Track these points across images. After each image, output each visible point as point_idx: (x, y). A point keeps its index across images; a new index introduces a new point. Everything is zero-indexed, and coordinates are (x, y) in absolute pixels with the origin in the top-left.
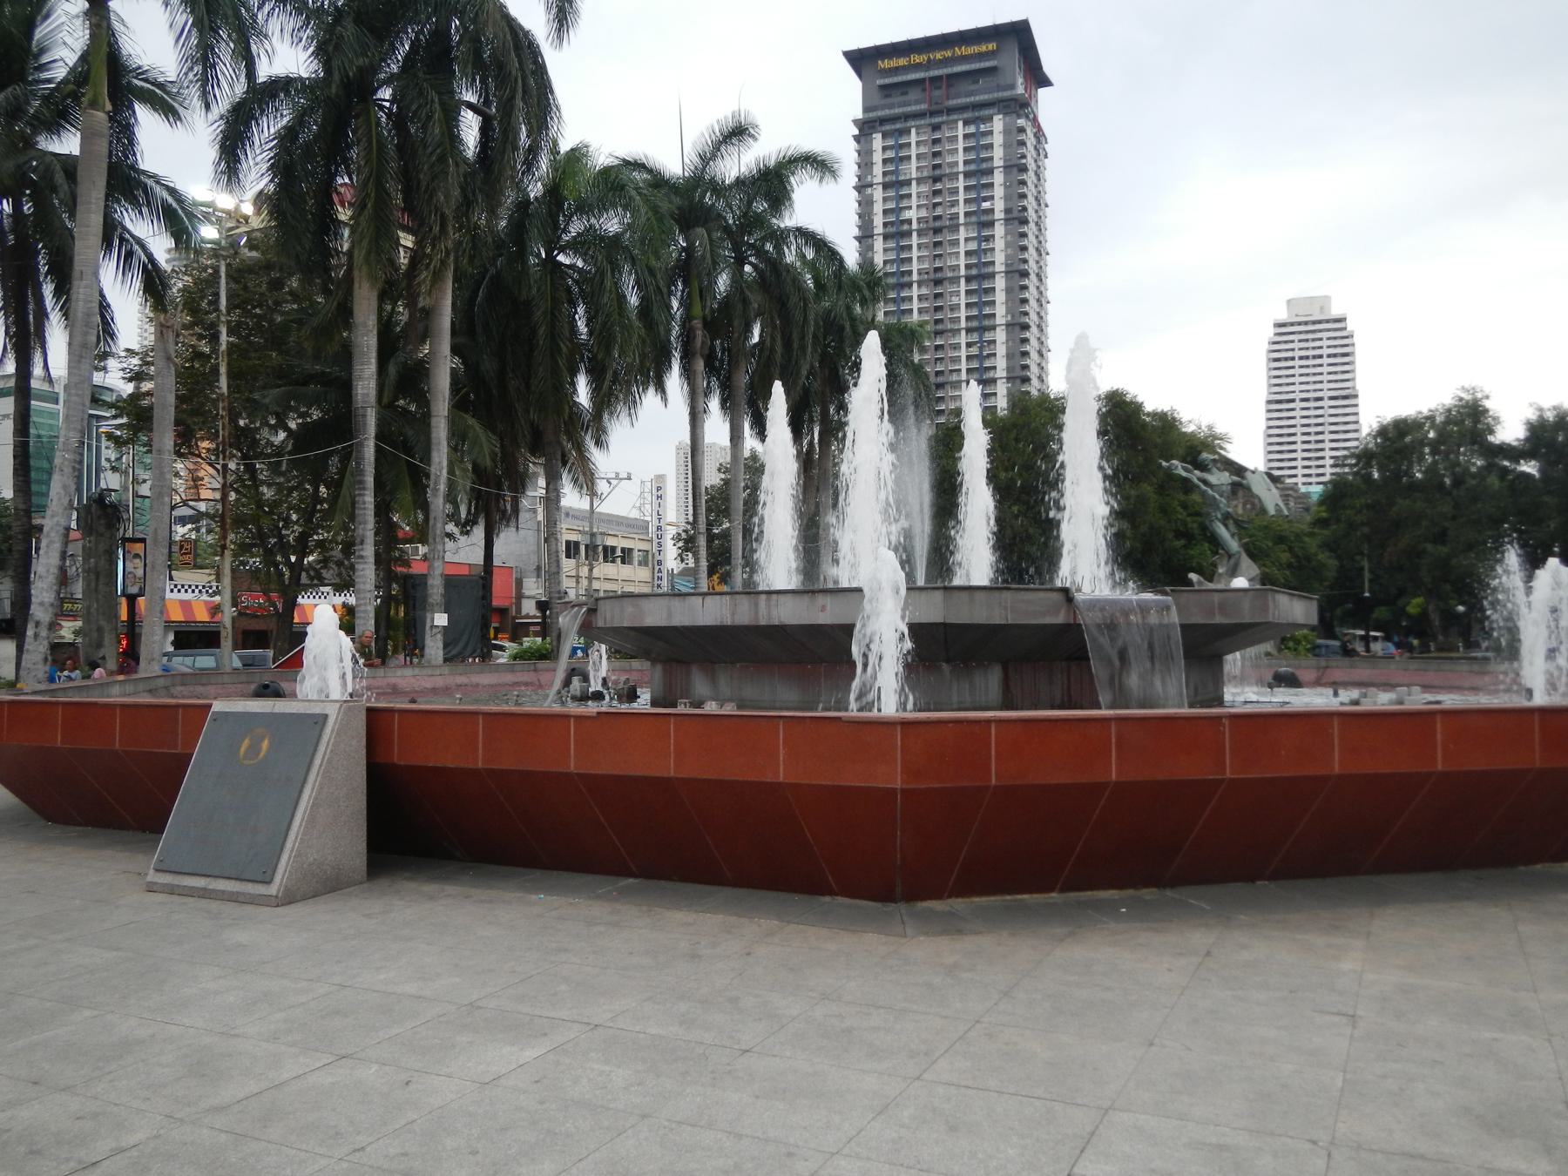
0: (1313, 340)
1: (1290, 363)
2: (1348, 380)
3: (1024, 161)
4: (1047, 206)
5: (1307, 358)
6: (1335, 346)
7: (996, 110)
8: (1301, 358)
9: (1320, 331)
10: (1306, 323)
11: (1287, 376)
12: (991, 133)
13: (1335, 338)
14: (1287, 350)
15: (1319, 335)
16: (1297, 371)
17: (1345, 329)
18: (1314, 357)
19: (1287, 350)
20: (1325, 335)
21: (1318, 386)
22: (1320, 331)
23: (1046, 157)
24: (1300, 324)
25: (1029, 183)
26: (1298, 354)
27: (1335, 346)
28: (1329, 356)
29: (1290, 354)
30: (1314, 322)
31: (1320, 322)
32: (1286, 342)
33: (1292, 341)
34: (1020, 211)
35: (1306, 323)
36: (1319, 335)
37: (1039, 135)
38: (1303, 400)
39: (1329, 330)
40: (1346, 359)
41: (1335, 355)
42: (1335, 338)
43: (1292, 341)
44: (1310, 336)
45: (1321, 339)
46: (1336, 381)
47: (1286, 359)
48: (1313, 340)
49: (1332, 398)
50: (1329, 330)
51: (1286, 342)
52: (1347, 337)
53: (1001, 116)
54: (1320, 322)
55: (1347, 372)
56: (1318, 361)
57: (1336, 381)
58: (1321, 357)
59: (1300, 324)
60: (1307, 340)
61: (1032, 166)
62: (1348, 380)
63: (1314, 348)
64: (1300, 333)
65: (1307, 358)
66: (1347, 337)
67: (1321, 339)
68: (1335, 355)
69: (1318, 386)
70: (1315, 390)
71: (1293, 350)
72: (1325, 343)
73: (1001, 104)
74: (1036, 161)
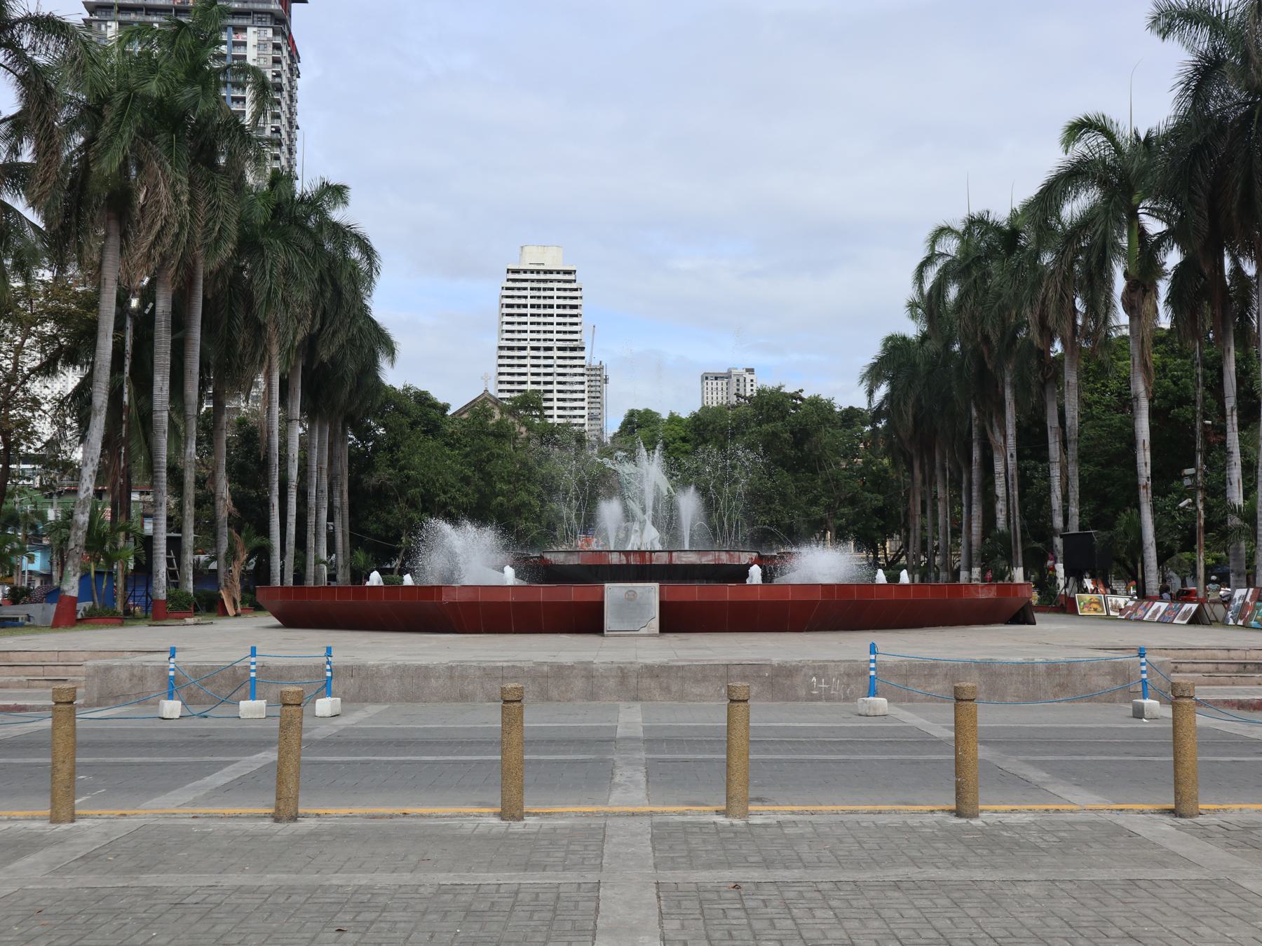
0: (545, 289)
1: (523, 311)
2: (576, 332)
3: (277, 80)
4: (297, 128)
5: (539, 306)
6: (565, 298)
7: (250, 22)
8: (533, 306)
9: (551, 281)
10: (538, 272)
11: (519, 323)
12: (244, 44)
13: (565, 290)
14: (519, 297)
15: (549, 285)
16: (529, 319)
17: (575, 281)
18: (545, 306)
19: (519, 297)
20: (556, 285)
21: (548, 336)
22: (551, 281)
23: (299, 77)
24: (532, 272)
25: (283, 104)
26: (530, 301)
27: (565, 298)
28: (558, 307)
29: (523, 301)
30: (546, 272)
31: (551, 272)
32: (519, 289)
33: (525, 289)
34: (272, 131)
35: (538, 272)
36: (549, 285)
37: (294, 56)
38: (533, 348)
39: (559, 281)
40: (574, 312)
41: (564, 307)
42: (565, 290)
43: (525, 289)
44: (542, 285)
45: (552, 289)
46: (565, 332)
47: (519, 306)
48: (545, 289)
49: (560, 349)
50: (559, 281)
51: (519, 289)
52: (576, 290)
53: (255, 29)
54: (551, 272)
55: (576, 324)
56: (549, 311)
57: (565, 332)
58: (551, 306)
59: (532, 272)
60: (539, 289)
61: (286, 87)
62: (576, 332)
63: (545, 297)
64: (533, 281)
65: (539, 306)
66: (576, 290)
67: (552, 289)
68: (564, 307)
69: (548, 336)
70: (545, 340)
71: (526, 297)
72: (556, 293)
73: (255, 15)
74: (290, 82)
